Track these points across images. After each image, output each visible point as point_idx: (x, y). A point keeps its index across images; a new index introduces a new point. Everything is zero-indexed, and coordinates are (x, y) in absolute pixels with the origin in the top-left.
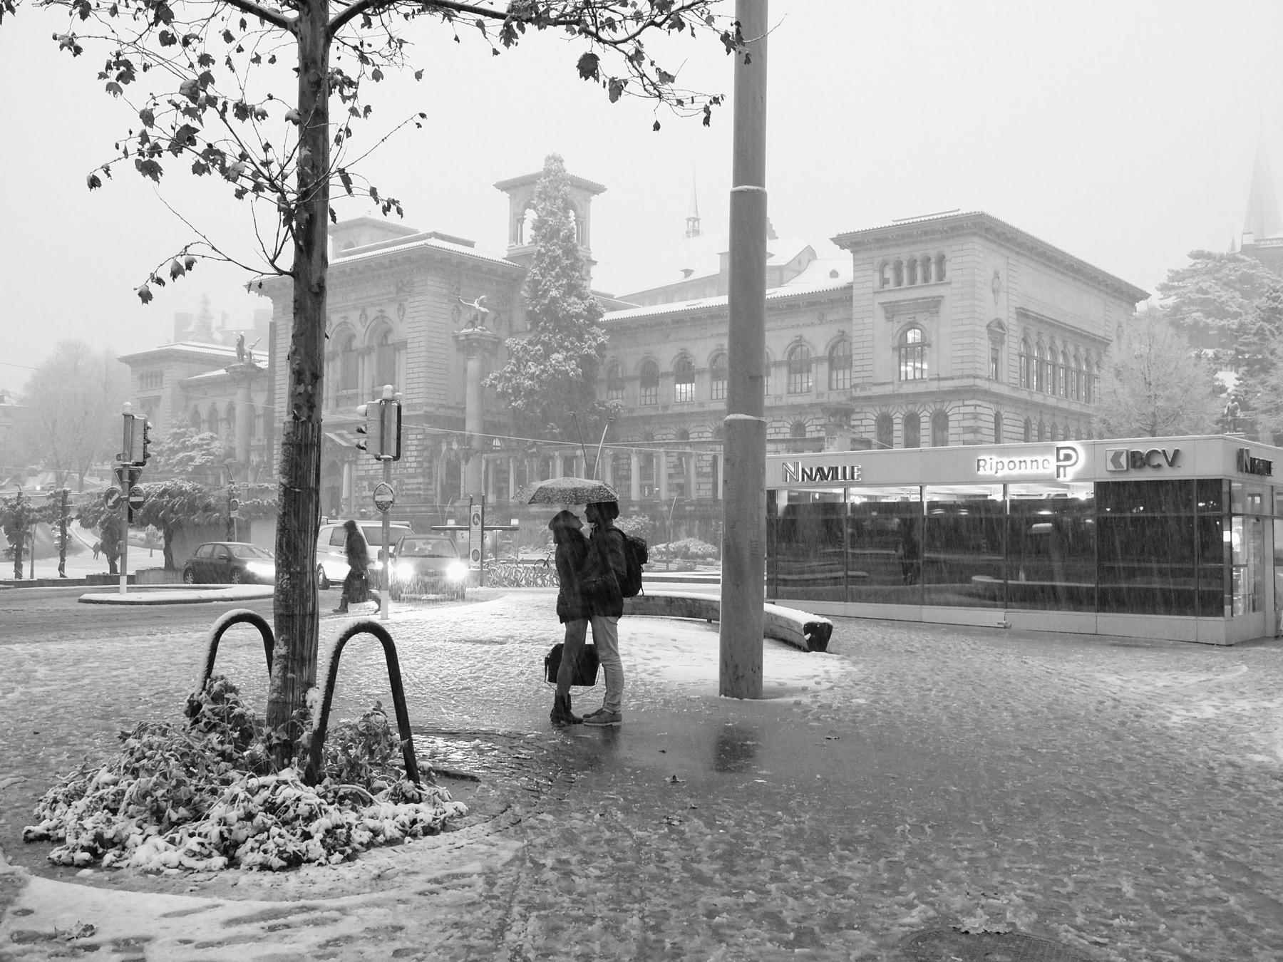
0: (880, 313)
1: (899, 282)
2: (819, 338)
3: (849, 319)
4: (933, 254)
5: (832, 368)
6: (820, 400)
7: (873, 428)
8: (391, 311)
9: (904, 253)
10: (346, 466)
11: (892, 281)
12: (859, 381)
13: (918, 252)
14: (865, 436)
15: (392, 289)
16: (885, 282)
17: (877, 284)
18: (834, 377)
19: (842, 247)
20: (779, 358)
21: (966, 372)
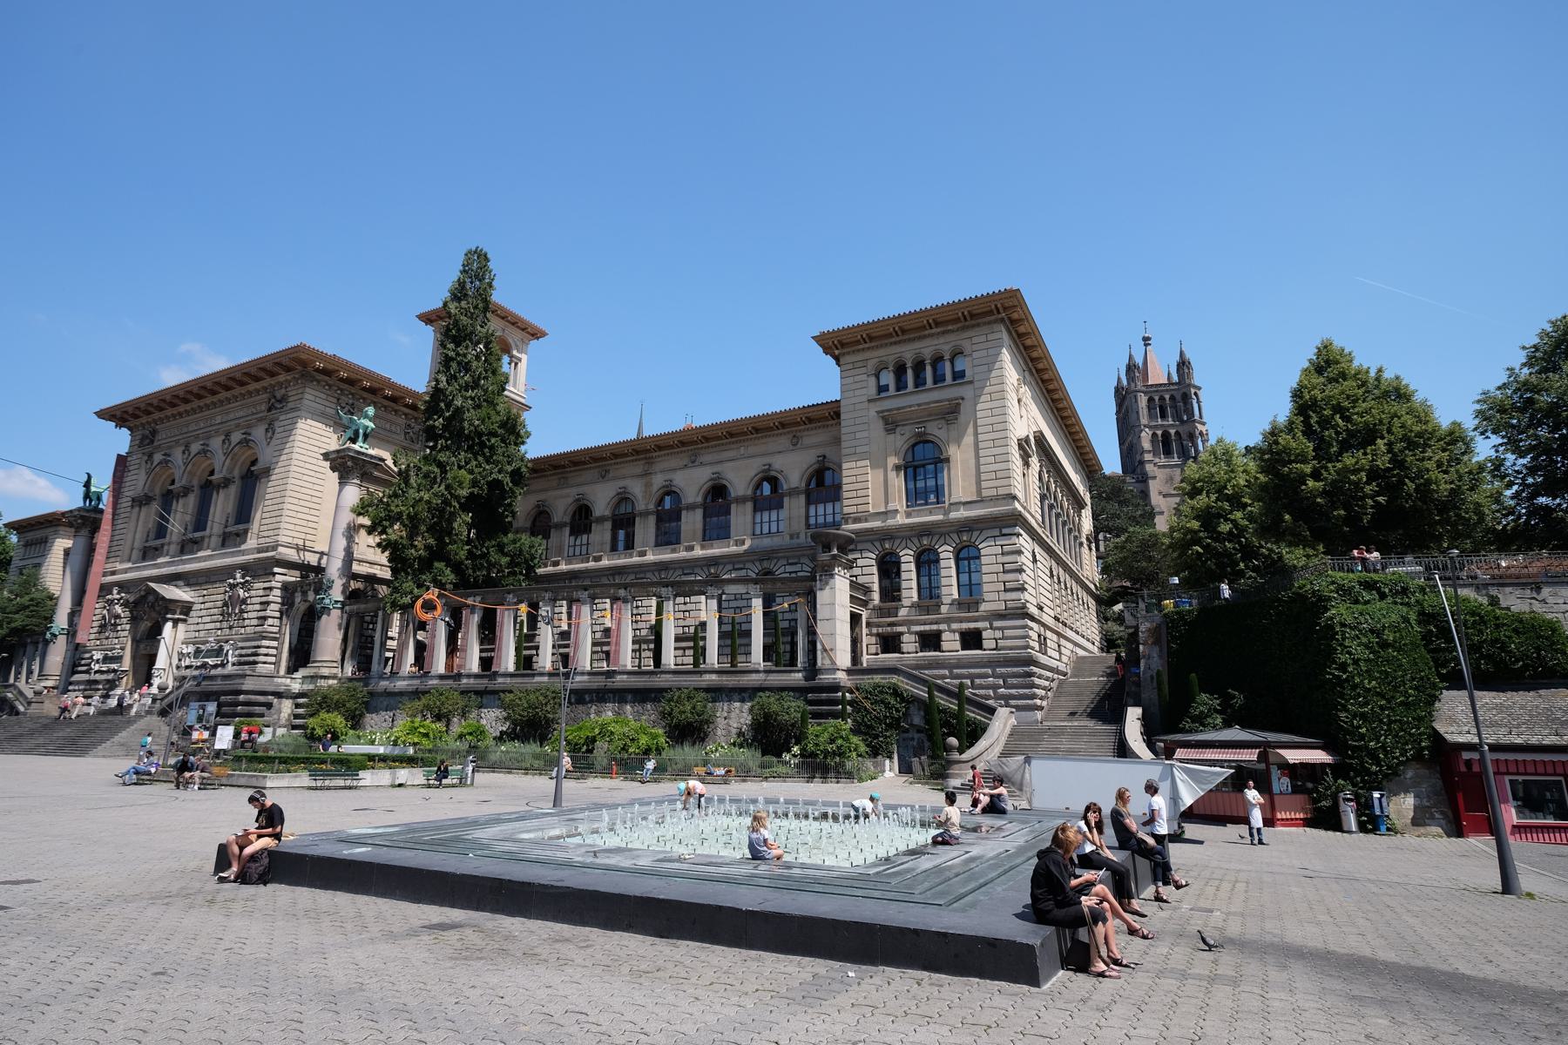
0: (878, 426)
1: (901, 385)
2: (794, 467)
3: (837, 441)
4: (946, 350)
5: (808, 503)
6: (795, 541)
7: (875, 570)
8: (259, 433)
9: (908, 352)
10: (169, 625)
11: (892, 387)
12: (854, 509)
13: (927, 348)
14: (861, 580)
15: (263, 407)
16: (882, 389)
17: (873, 390)
18: (812, 512)
19: (827, 351)
20: (741, 492)
21: (1002, 491)
